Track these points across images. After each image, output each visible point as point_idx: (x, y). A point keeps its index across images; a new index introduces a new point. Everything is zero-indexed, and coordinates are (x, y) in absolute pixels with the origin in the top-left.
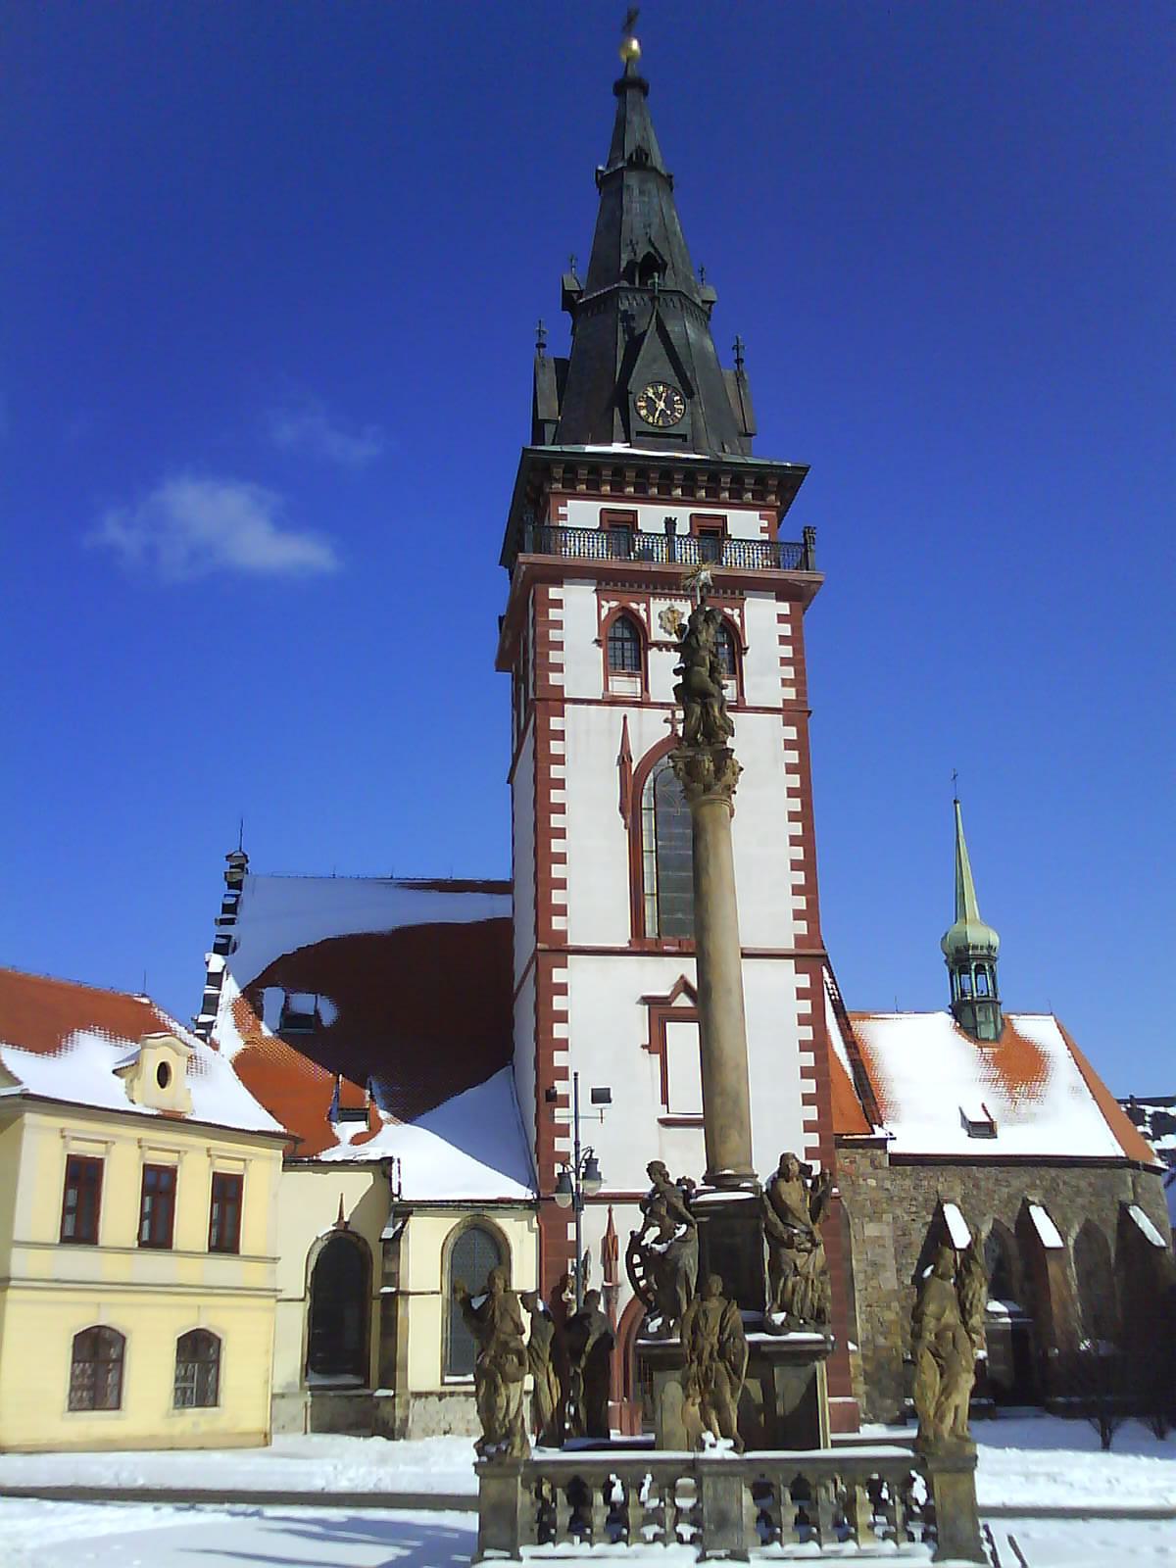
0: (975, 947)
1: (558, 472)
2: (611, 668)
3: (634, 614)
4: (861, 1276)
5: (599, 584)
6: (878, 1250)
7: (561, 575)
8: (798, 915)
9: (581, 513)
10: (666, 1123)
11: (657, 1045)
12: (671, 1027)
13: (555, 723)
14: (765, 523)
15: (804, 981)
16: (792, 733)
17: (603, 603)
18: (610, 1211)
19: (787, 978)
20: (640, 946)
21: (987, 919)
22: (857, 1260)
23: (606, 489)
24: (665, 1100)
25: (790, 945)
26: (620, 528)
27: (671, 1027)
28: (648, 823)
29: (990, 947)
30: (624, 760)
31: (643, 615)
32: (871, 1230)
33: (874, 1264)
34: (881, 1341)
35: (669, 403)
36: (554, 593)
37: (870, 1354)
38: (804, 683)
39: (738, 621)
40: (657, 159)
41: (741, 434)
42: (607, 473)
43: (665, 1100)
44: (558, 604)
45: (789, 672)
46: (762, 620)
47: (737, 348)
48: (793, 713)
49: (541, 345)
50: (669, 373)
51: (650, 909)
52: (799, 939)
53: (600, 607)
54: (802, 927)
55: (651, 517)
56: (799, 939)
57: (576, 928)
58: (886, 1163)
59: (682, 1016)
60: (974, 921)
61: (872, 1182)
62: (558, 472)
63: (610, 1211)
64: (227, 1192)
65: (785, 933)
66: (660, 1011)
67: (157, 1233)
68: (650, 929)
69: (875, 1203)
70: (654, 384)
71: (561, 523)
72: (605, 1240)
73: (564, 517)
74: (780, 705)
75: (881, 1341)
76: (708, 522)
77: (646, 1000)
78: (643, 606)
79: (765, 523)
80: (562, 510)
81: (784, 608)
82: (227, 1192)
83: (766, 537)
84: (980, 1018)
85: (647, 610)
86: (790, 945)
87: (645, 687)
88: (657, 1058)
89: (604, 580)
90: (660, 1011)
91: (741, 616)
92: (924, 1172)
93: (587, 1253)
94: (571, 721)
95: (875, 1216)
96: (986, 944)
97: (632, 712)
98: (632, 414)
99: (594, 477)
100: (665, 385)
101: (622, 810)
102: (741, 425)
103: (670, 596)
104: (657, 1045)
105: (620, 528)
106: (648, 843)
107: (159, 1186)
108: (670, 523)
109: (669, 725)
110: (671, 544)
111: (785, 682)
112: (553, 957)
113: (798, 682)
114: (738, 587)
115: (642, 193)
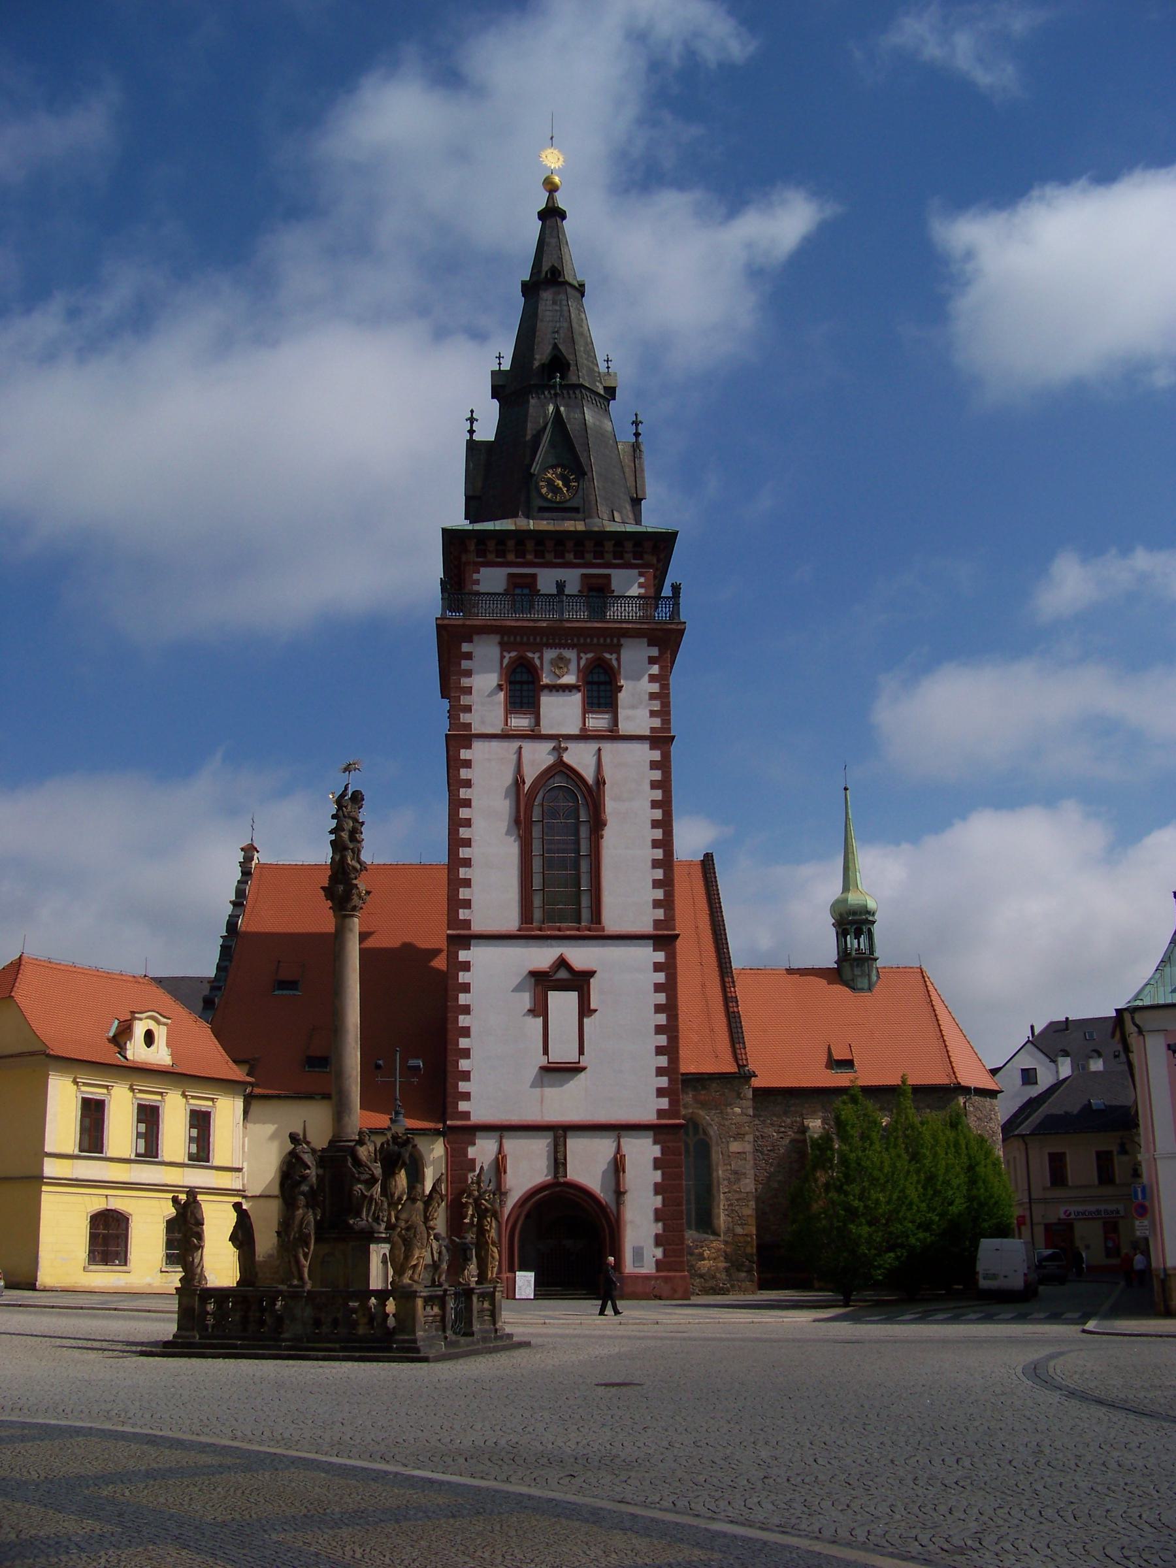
4: (726, 1182)
5: (502, 638)
6: (740, 1162)
9: (491, 579)
11: (540, 1009)
15: (660, 957)
16: (656, 755)
17: (505, 654)
22: (724, 1171)
23: (511, 557)
24: (546, 1052)
26: (522, 588)
28: (536, 831)
30: (518, 782)
31: (537, 662)
32: (735, 1147)
33: (736, 1173)
36: (466, 647)
37: (730, 1240)
38: (668, 713)
39: (615, 663)
42: (511, 543)
43: (546, 1052)
48: (661, 740)
51: (537, 901)
53: (502, 657)
54: (660, 914)
55: (547, 579)
56: (657, 923)
57: (481, 918)
58: (750, 1094)
61: (738, 1110)
65: (644, 920)
67: (150, 1151)
68: (537, 914)
69: (739, 1126)
71: (476, 588)
73: (477, 582)
74: (647, 733)
75: (739, 1230)
78: (537, 655)
80: (475, 576)
81: (654, 652)
85: (541, 658)
86: (648, 929)
90: (543, 982)
91: (618, 660)
95: (739, 1136)
102: (633, 491)
104: (540, 1009)
105: (522, 588)
106: (537, 849)
108: (561, 586)
113: (664, 713)
114: (615, 637)
115: (554, 303)
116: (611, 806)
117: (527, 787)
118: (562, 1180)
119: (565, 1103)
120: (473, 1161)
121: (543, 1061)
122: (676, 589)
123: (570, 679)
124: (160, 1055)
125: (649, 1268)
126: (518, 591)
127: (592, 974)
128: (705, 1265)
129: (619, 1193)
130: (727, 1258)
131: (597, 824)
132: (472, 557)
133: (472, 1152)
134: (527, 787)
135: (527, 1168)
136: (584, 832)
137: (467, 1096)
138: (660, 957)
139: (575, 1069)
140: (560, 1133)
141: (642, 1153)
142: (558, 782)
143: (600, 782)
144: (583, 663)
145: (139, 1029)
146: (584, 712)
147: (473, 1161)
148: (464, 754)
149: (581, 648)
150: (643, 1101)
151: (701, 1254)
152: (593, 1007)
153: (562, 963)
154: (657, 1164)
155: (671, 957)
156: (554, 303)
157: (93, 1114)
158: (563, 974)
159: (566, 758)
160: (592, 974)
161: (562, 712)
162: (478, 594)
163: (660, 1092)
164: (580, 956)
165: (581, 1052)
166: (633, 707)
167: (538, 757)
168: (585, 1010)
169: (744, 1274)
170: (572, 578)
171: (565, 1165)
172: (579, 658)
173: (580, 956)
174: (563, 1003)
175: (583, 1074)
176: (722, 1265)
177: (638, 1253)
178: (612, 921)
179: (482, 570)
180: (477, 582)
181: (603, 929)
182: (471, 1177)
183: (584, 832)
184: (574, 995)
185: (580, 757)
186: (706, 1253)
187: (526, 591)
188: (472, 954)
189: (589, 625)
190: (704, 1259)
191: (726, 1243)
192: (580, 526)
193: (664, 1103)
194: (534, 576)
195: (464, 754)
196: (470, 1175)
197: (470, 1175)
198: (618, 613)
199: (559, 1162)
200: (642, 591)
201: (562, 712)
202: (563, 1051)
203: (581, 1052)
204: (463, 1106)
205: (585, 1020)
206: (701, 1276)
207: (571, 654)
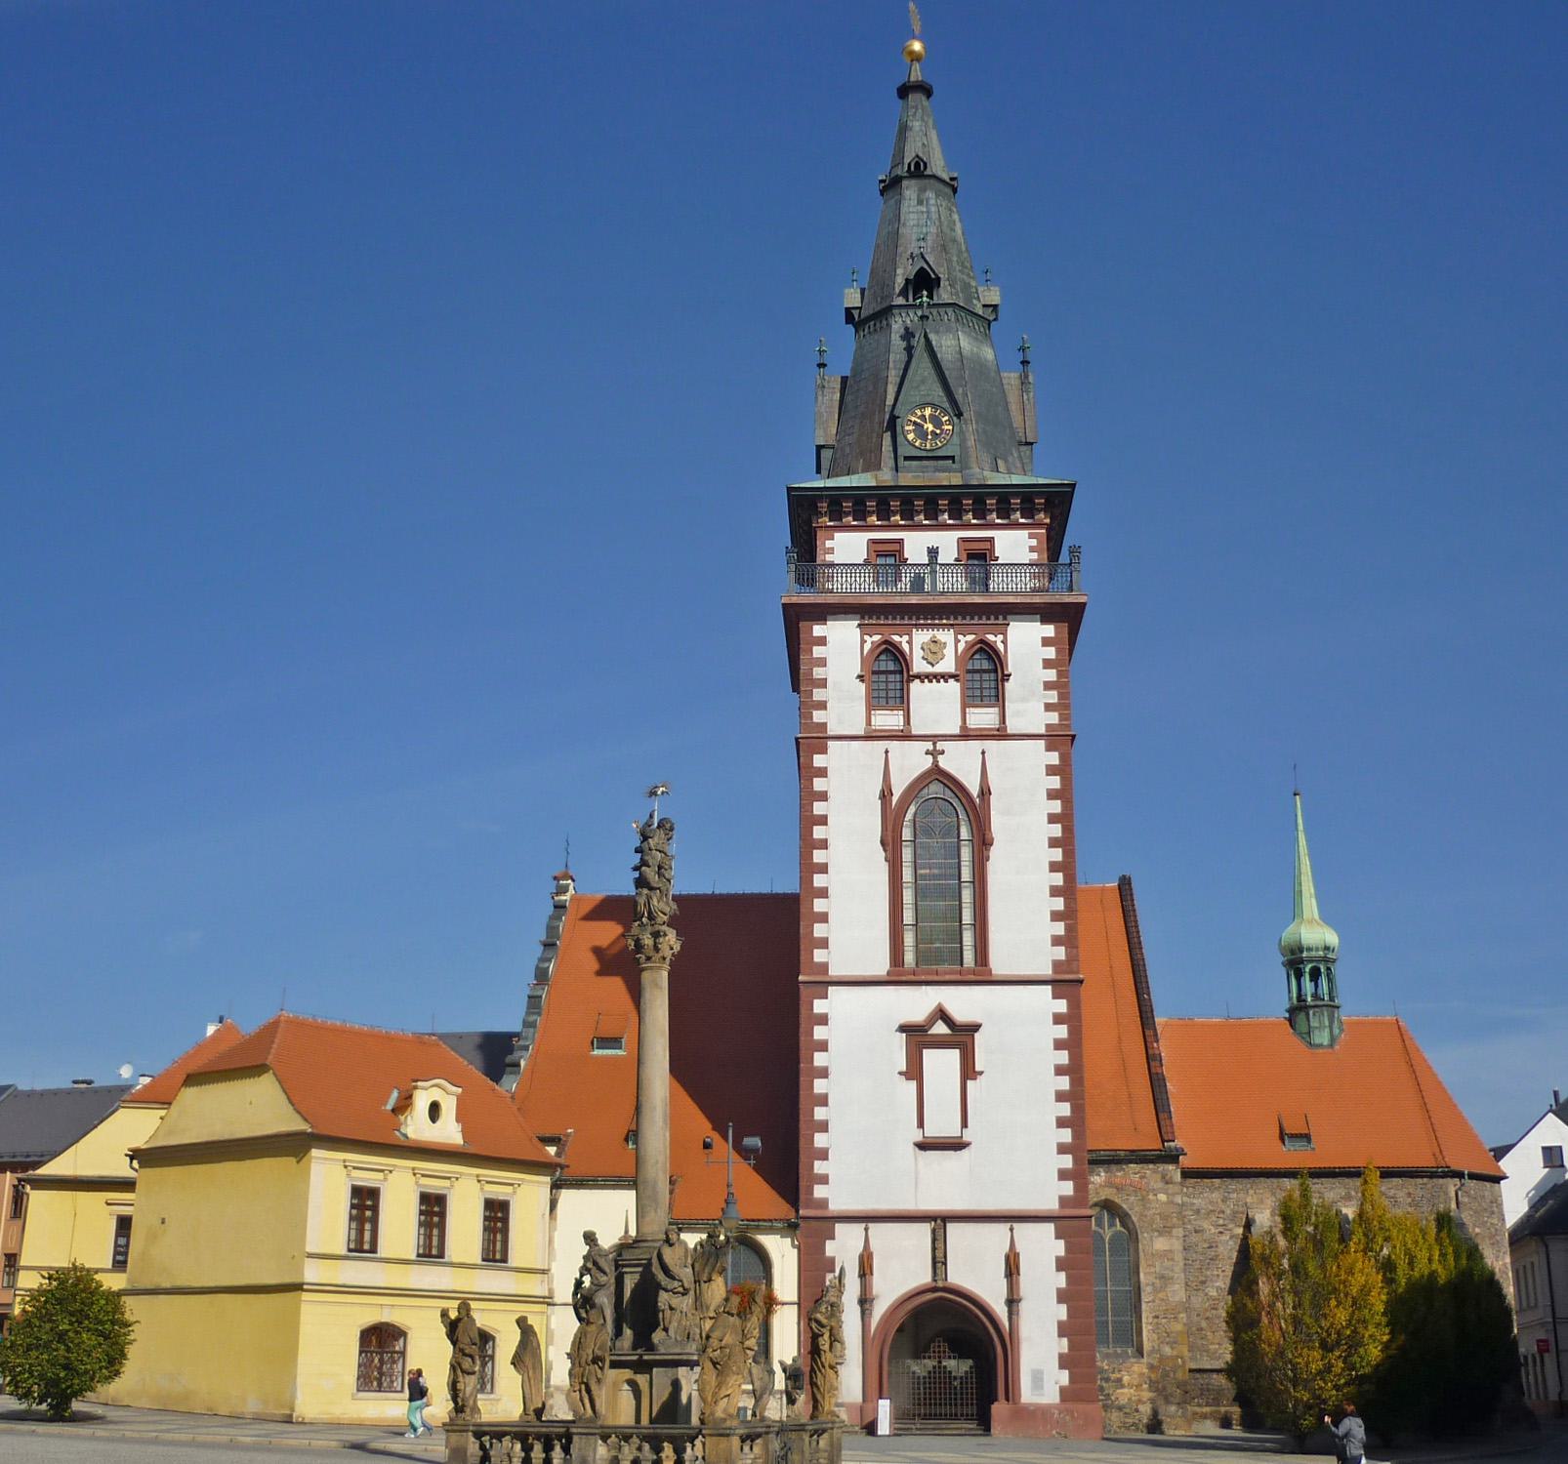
0: (1309, 949)
1: (824, 506)
2: (874, 702)
4: (1149, 1289)
6: (1167, 1263)
7: (824, 612)
8: (1057, 941)
9: (846, 546)
10: (923, 1146)
11: (914, 1071)
12: (929, 1055)
14: (1034, 542)
15: (1062, 1006)
16: (1054, 758)
19: (1045, 1003)
20: (898, 977)
21: (1327, 918)
24: (921, 1124)
25: (1047, 971)
26: (888, 556)
27: (929, 1055)
28: (907, 854)
29: (1327, 948)
30: (885, 795)
31: (906, 647)
32: (1160, 1244)
33: (1162, 1277)
34: (1167, 1350)
35: (937, 423)
36: (818, 630)
38: (1067, 707)
39: (1000, 647)
40: (938, 166)
41: (1020, 444)
43: (921, 1124)
44: (822, 641)
45: (1053, 697)
46: (1026, 643)
47: (1023, 349)
48: (1055, 738)
49: (822, 365)
50: (938, 394)
51: (909, 939)
52: (1056, 965)
53: (863, 642)
54: (1060, 953)
55: (916, 545)
56: (1056, 965)
59: (940, 1043)
60: (1311, 922)
61: (1162, 1197)
62: (824, 506)
64: (497, 1214)
65: (1043, 959)
66: (917, 1037)
67: (432, 1250)
68: (909, 958)
69: (1165, 1217)
71: (829, 558)
72: (861, 1257)
73: (831, 551)
74: (1042, 731)
75: (1167, 1350)
77: (903, 1028)
78: (906, 638)
79: (1034, 542)
80: (829, 544)
81: (1049, 630)
82: (497, 1214)
84: (1314, 1023)
85: (910, 643)
86: (1047, 971)
87: (907, 721)
88: (913, 1084)
89: (865, 612)
90: (917, 1037)
91: (1004, 642)
92: (1233, 1184)
93: (842, 1269)
94: (834, 758)
95: (1165, 1231)
96: (1321, 945)
97: (893, 745)
98: (900, 439)
99: (854, 507)
100: (933, 406)
101: (883, 843)
103: (933, 626)
104: (914, 1071)
105: (888, 556)
106: (907, 875)
107: (433, 1208)
108: (933, 553)
110: (934, 572)
111: (1049, 707)
113: (1062, 706)
115: (920, 202)
116: (999, 823)
117: (895, 799)
118: (940, 1284)
119: (943, 1184)
120: (832, 1260)
122: (1074, 551)
123: (947, 665)
124: (448, 1132)
125: (1050, 1396)
126: (880, 561)
127: (976, 1027)
128: (1124, 1395)
129: (1012, 1302)
130: (1153, 1385)
131: (983, 842)
132: (825, 520)
133: (831, 1248)
134: (895, 799)
135: (902, 1269)
136: (966, 854)
137: (824, 1180)
138: (1062, 1006)
139: (957, 1145)
140: (940, 1222)
141: (1042, 1247)
142: (935, 789)
143: (985, 792)
144: (961, 646)
145: (422, 1100)
146: (964, 707)
148: (819, 761)
149: (960, 630)
150: (1045, 1185)
151: (1119, 1380)
152: (978, 1068)
153: (941, 1014)
154: (1061, 1264)
156: (920, 202)
157: (365, 1202)
158: (940, 1028)
159: (944, 763)
160: (976, 1027)
161: (936, 705)
162: (832, 565)
163: (1063, 1175)
164: (963, 1002)
165: (965, 1124)
166: (1024, 700)
167: (910, 761)
168: (968, 1071)
169: (1173, 1408)
170: (948, 543)
171: (945, 1264)
172: (957, 641)
174: (941, 1064)
175: (965, 1152)
176: (1146, 1395)
177: (1038, 1378)
180: (831, 551)
183: (966, 854)
184: (954, 1055)
185: (961, 762)
186: (1126, 1379)
187: (891, 561)
189: (969, 600)
190: (1122, 1386)
191: (1151, 1367)
192: (956, 480)
193: (1068, 1189)
194: (900, 542)
195: (819, 761)
196: (829, 1276)
197: (829, 1276)
198: (1004, 586)
199: (939, 1262)
200: (1035, 556)
201: (936, 705)
202: (942, 1122)
203: (965, 1124)
204: (819, 1192)
206: (1120, 1408)
207: (946, 636)
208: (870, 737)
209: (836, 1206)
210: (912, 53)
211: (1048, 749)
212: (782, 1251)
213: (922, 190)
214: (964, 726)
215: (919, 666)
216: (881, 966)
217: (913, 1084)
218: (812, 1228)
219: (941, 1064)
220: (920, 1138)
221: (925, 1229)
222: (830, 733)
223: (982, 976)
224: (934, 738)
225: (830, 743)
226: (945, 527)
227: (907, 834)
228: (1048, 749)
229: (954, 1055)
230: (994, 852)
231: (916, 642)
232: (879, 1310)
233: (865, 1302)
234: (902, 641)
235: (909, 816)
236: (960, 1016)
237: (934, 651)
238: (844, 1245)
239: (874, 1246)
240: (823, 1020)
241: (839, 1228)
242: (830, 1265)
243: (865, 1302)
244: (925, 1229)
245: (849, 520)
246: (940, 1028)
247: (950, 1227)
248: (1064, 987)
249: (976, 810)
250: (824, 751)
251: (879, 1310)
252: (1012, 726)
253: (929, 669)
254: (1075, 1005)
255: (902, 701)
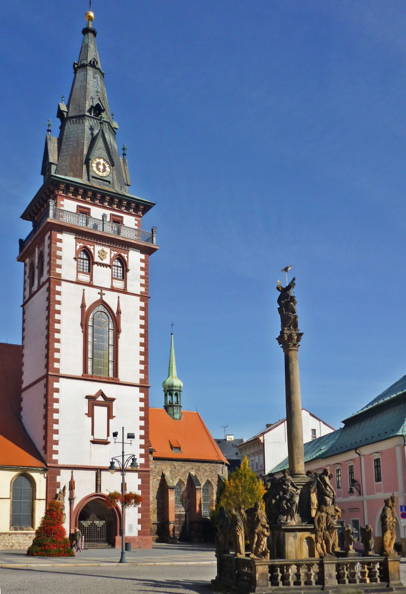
0: (175, 387)
3: (89, 250)
8: (141, 372)
11: (91, 414)
12: (96, 408)
13: (58, 288)
18: (72, 472)
20: (85, 378)
21: (179, 377)
24: (93, 434)
25: (138, 382)
27: (96, 408)
28: (90, 331)
29: (180, 387)
30: (83, 306)
31: (92, 251)
39: (126, 259)
40: (99, 66)
43: (93, 434)
45: (143, 281)
46: (135, 258)
48: (143, 297)
49: (49, 131)
50: (105, 154)
51: (90, 363)
52: (141, 380)
53: (76, 245)
54: (142, 376)
55: (97, 212)
56: (141, 380)
59: (100, 404)
63: (72, 472)
65: (137, 378)
66: (92, 400)
70: (100, 158)
71: (62, 208)
73: (62, 206)
74: (139, 293)
76: (116, 218)
77: (87, 397)
78: (92, 247)
81: (143, 256)
83: (137, 228)
86: (138, 382)
88: (90, 419)
90: (92, 400)
94: (63, 288)
96: (179, 386)
97: (86, 288)
98: (90, 168)
100: (104, 160)
101: (82, 325)
104: (91, 414)
106: (90, 339)
109: (100, 296)
112: (55, 378)
116: (123, 325)
117: (86, 309)
120: (59, 483)
121: (91, 438)
123: (107, 261)
127: (113, 400)
131: (117, 331)
132: (61, 192)
133: (59, 479)
134: (86, 309)
135: (85, 488)
137: (56, 452)
138: (142, 395)
140: (98, 470)
143: (119, 312)
144: (112, 255)
147: (59, 483)
152: (114, 415)
153: (102, 394)
155: (147, 395)
159: (105, 298)
160: (113, 400)
161: (102, 276)
164: (110, 390)
167: (92, 296)
168: (110, 416)
171: (100, 486)
172: (111, 253)
173: (110, 390)
174: (101, 412)
175: (108, 445)
178: (122, 377)
179: (65, 200)
181: (119, 380)
182: (58, 491)
184: (105, 409)
185: (111, 299)
188: (61, 384)
195: (58, 288)
198: (127, 235)
201: (102, 276)
202: (101, 434)
204: (55, 457)
205: (110, 420)
207: (107, 250)
208: (78, 283)
209: (61, 463)
210: (89, 16)
211: (141, 300)
212: (40, 479)
213: (95, 73)
214: (112, 286)
215: (97, 259)
216: (79, 372)
217: (90, 419)
218: (51, 470)
219: (101, 412)
220: (92, 439)
221: (93, 473)
222: (62, 278)
223: (115, 380)
224: (102, 288)
225: (62, 282)
226: (105, 208)
227: (90, 323)
228: (141, 300)
229: (105, 409)
230: (121, 335)
231: (96, 249)
232: (76, 502)
233: (71, 499)
234: (91, 248)
235: (91, 316)
236: (108, 395)
237: (102, 255)
238: (64, 478)
239: (75, 479)
240: (57, 390)
241: (62, 471)
242: (58, 485)
243: (71, 499)
244: (93, 473)
245: (70, 195)
246: (100, 399)
247: (103, 473)
248: (143, 389)
249: (116, 318)
250: (60, 285)
251: (76, 502)
252: (129, 290)
253: (100, 261)
254: (147, 395)
255: (90, 271)
